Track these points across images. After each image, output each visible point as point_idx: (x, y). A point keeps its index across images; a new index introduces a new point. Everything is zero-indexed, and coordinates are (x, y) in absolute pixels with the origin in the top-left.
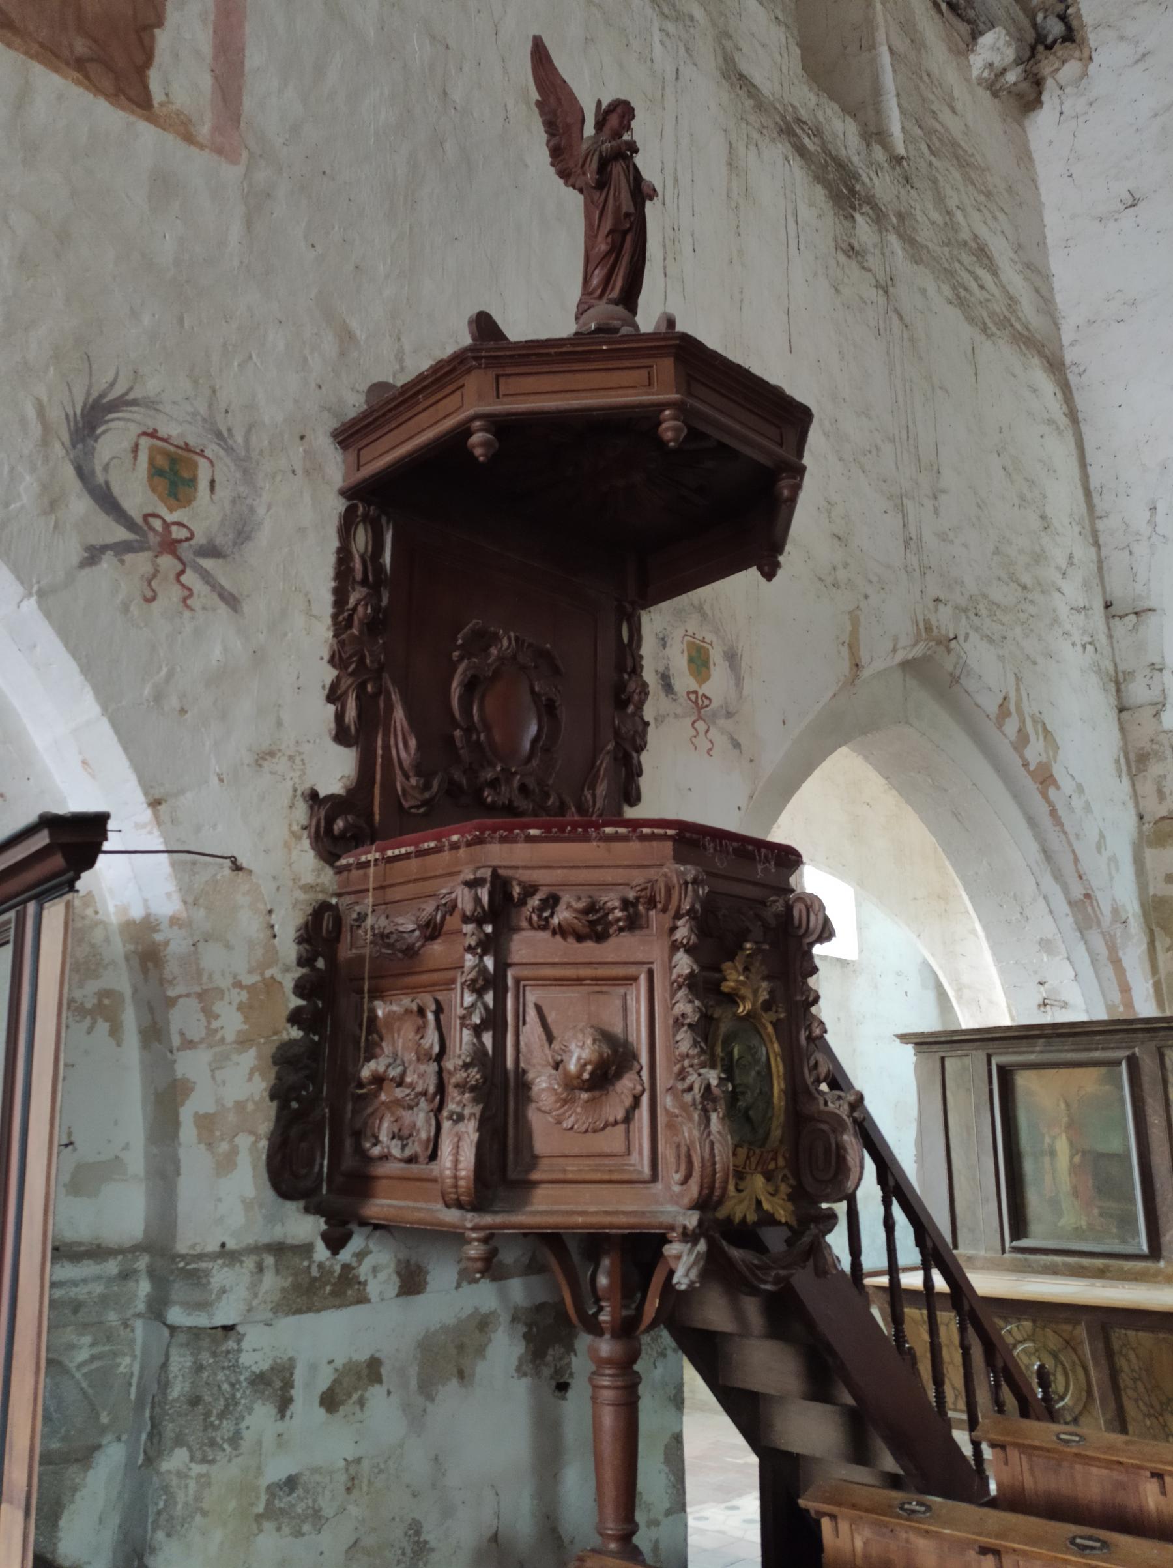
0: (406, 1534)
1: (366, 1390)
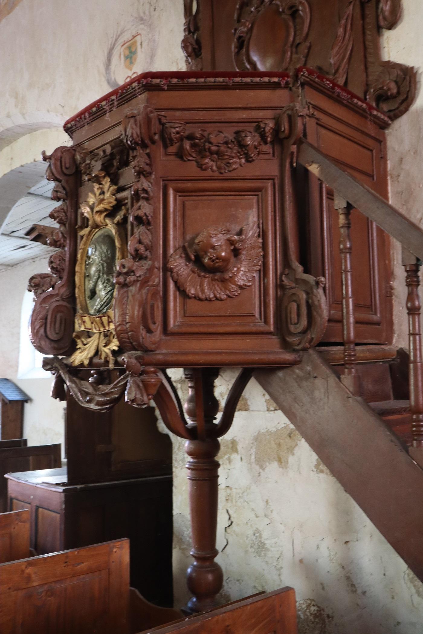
0: (254, 534)
1: (231, 454)
